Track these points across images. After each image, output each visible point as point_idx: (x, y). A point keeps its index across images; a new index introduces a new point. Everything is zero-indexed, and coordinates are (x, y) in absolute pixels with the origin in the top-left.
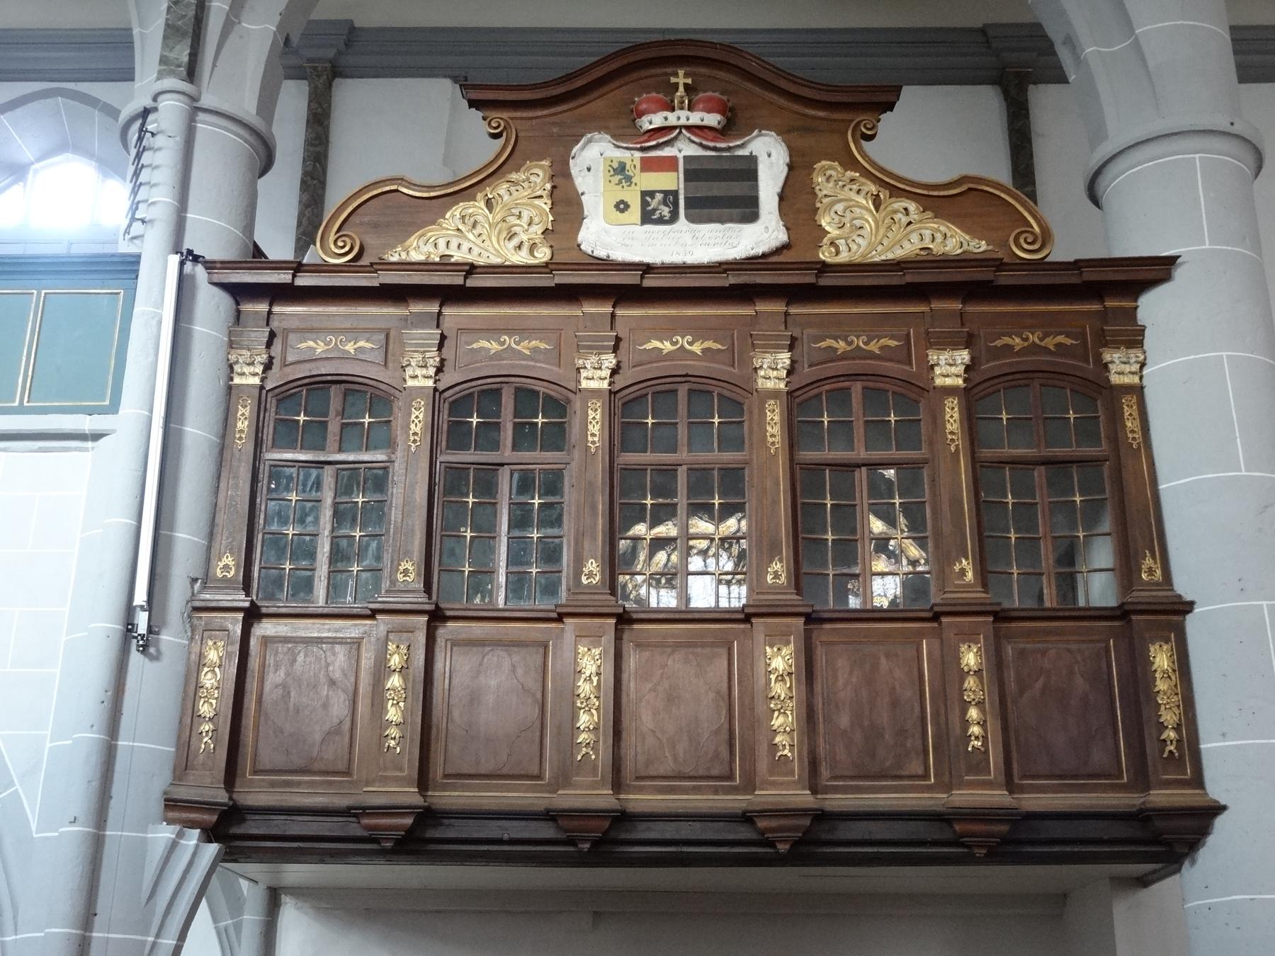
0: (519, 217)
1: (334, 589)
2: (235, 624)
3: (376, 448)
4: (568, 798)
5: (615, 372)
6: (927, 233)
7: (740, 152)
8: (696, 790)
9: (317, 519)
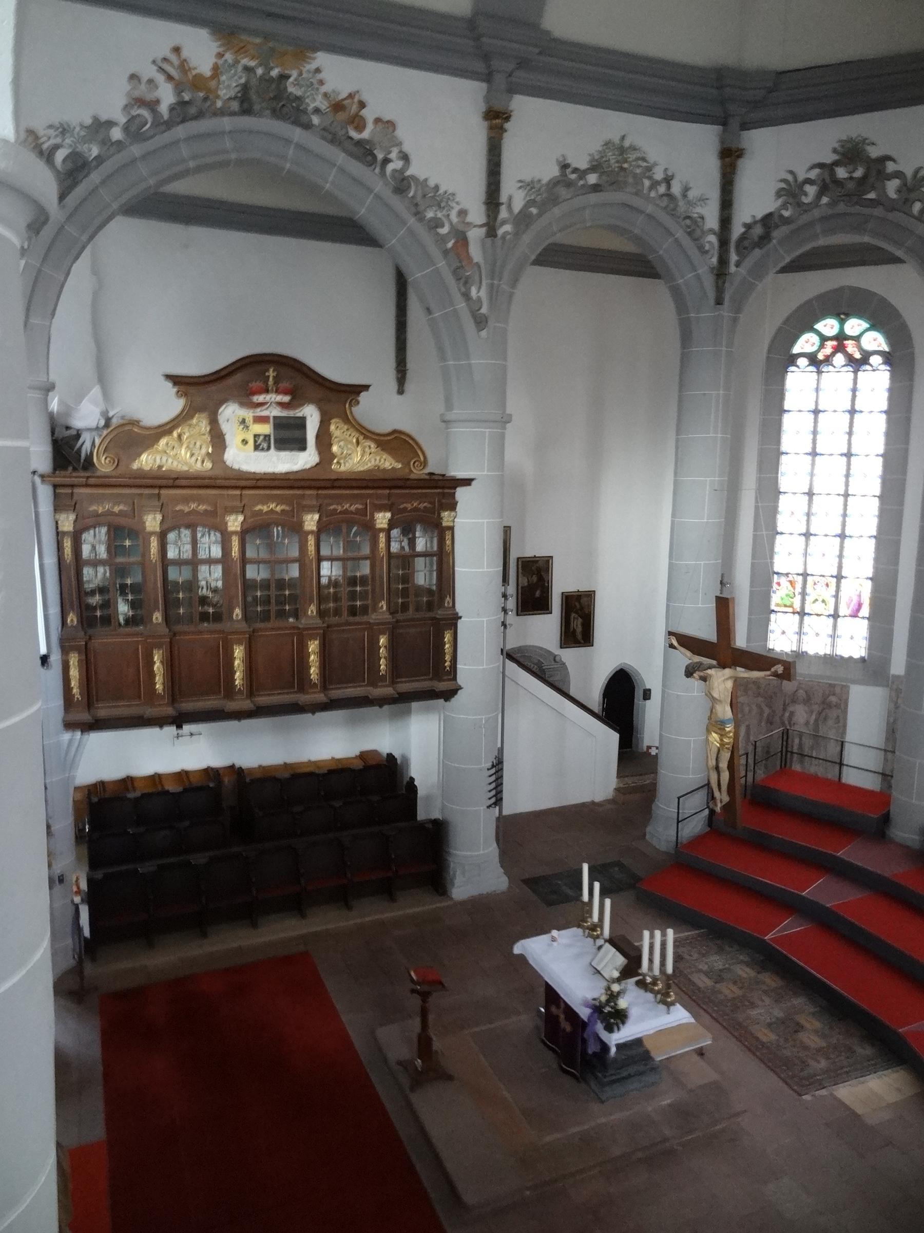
6: (378, 458)
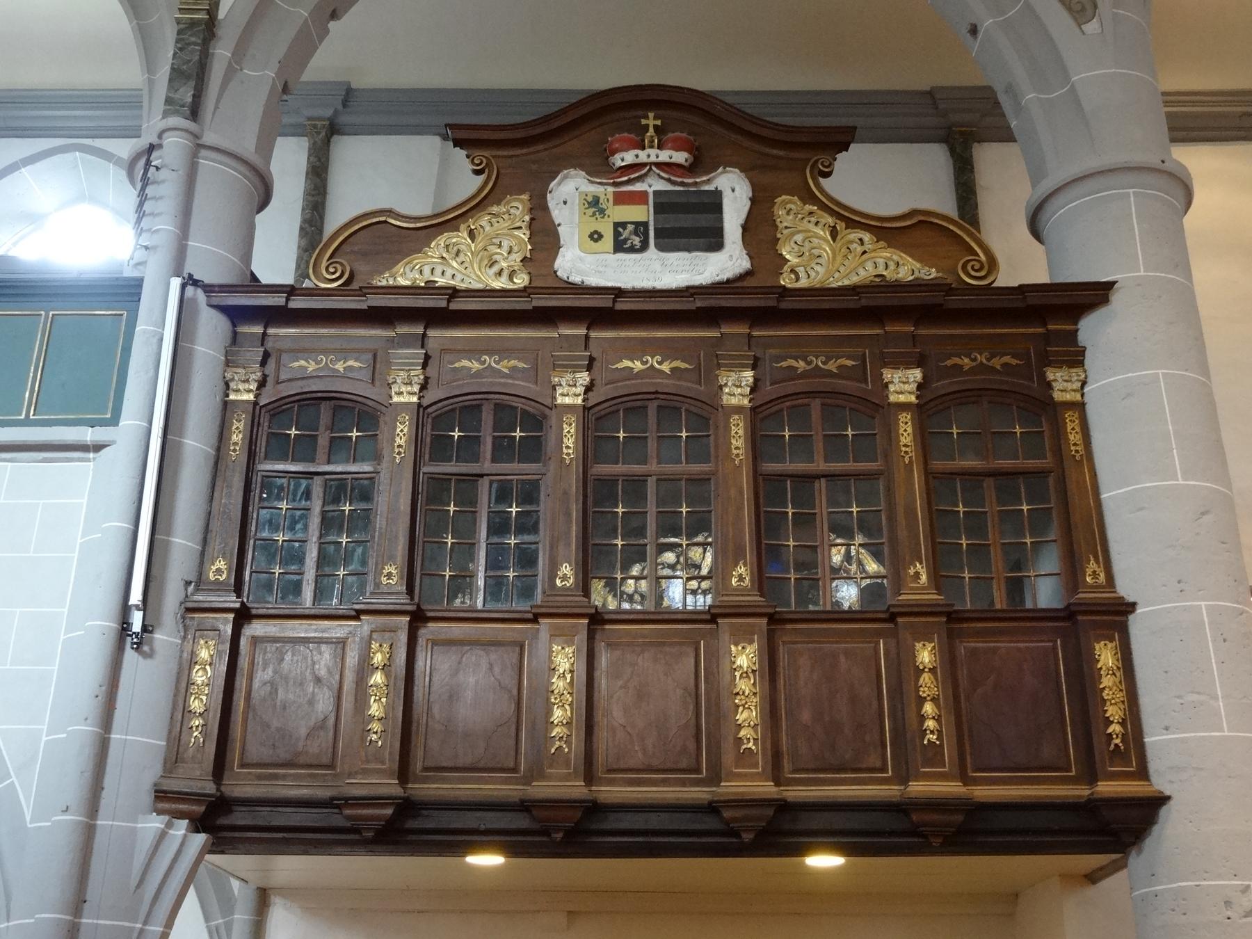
0: (500, 246)
1: (321, 593)
2: (226, 624)
3: (363, 460)
4: (542, 789)
5: (589, 389)
6: (881, 262)
7: (706, 188)
8: (665, 782)
9: (306, 527)
